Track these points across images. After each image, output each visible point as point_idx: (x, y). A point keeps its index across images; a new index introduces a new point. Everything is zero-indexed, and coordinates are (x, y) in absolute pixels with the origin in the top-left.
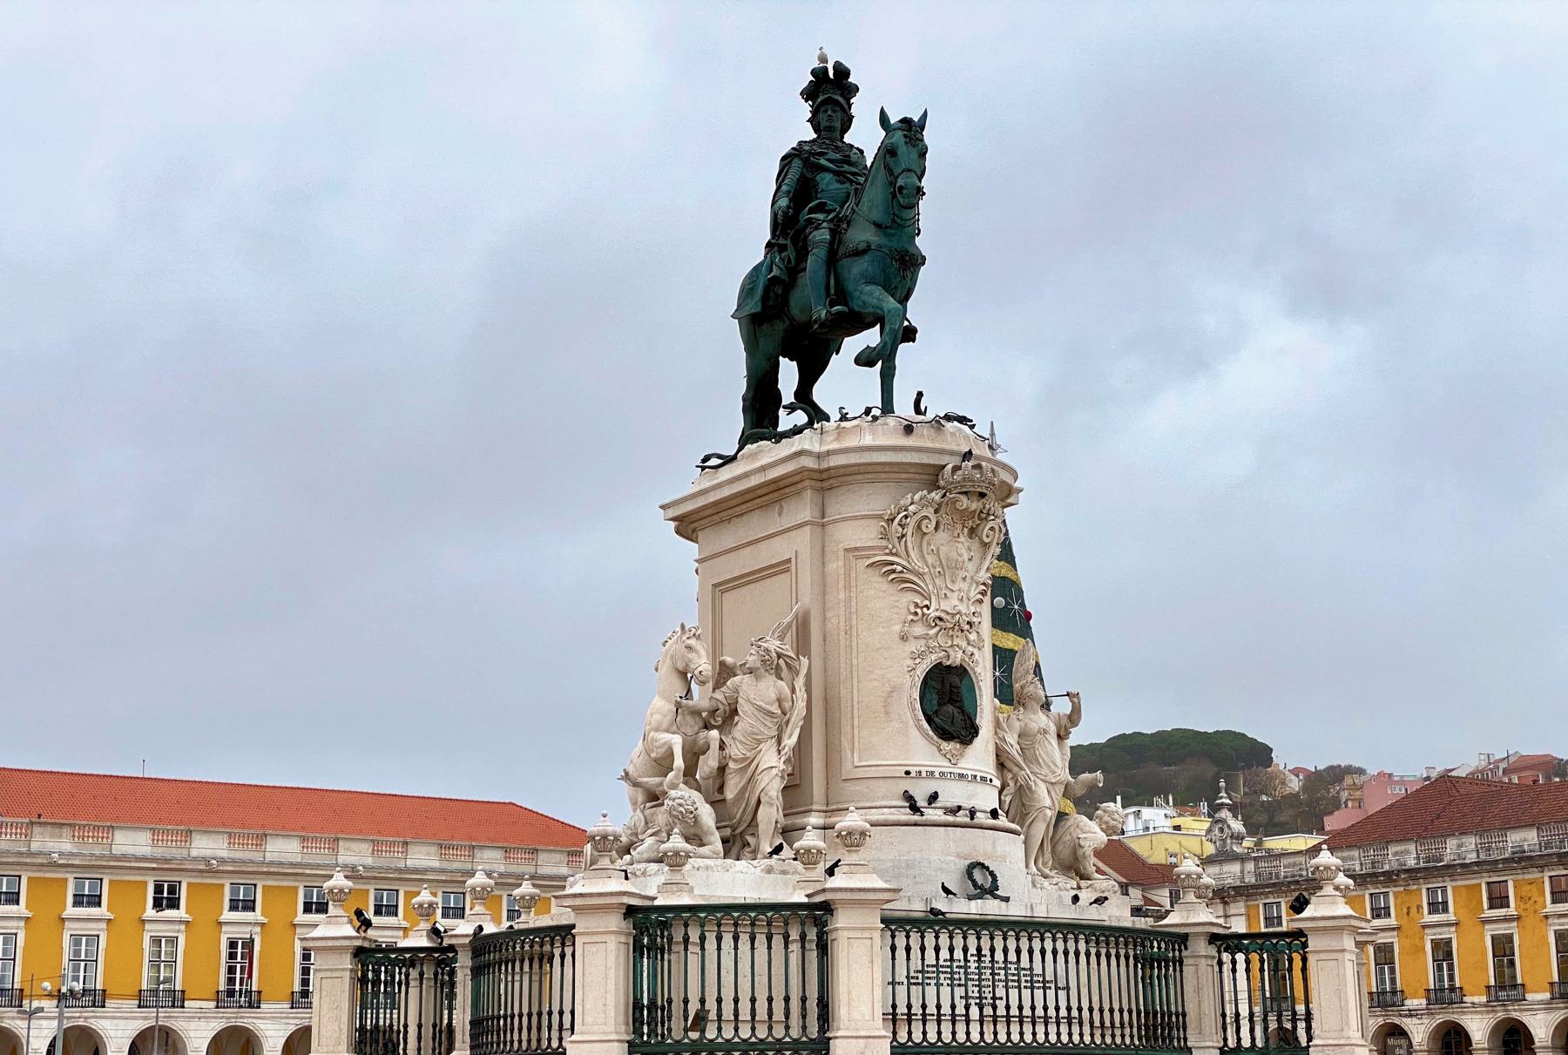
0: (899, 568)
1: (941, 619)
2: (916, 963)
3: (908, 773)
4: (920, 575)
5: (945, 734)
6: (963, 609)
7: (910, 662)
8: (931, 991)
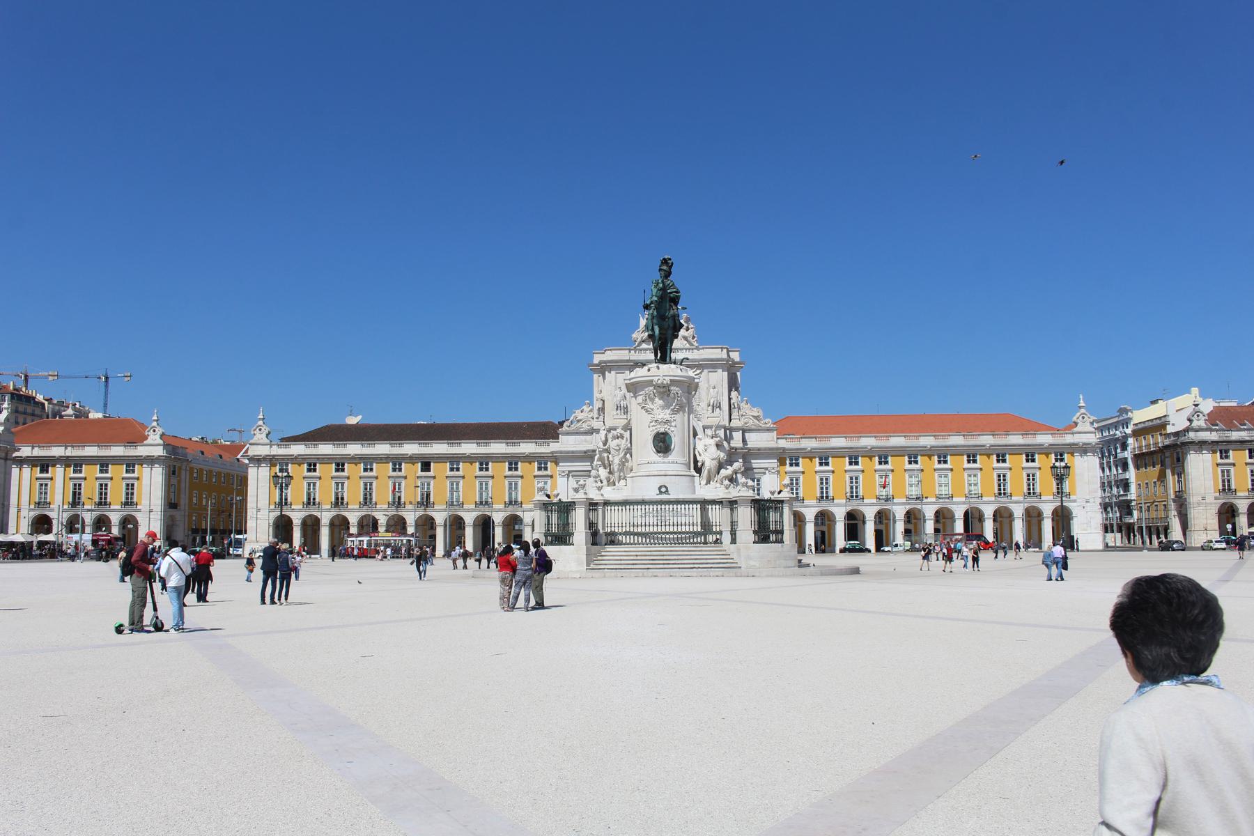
5: (658, 452)
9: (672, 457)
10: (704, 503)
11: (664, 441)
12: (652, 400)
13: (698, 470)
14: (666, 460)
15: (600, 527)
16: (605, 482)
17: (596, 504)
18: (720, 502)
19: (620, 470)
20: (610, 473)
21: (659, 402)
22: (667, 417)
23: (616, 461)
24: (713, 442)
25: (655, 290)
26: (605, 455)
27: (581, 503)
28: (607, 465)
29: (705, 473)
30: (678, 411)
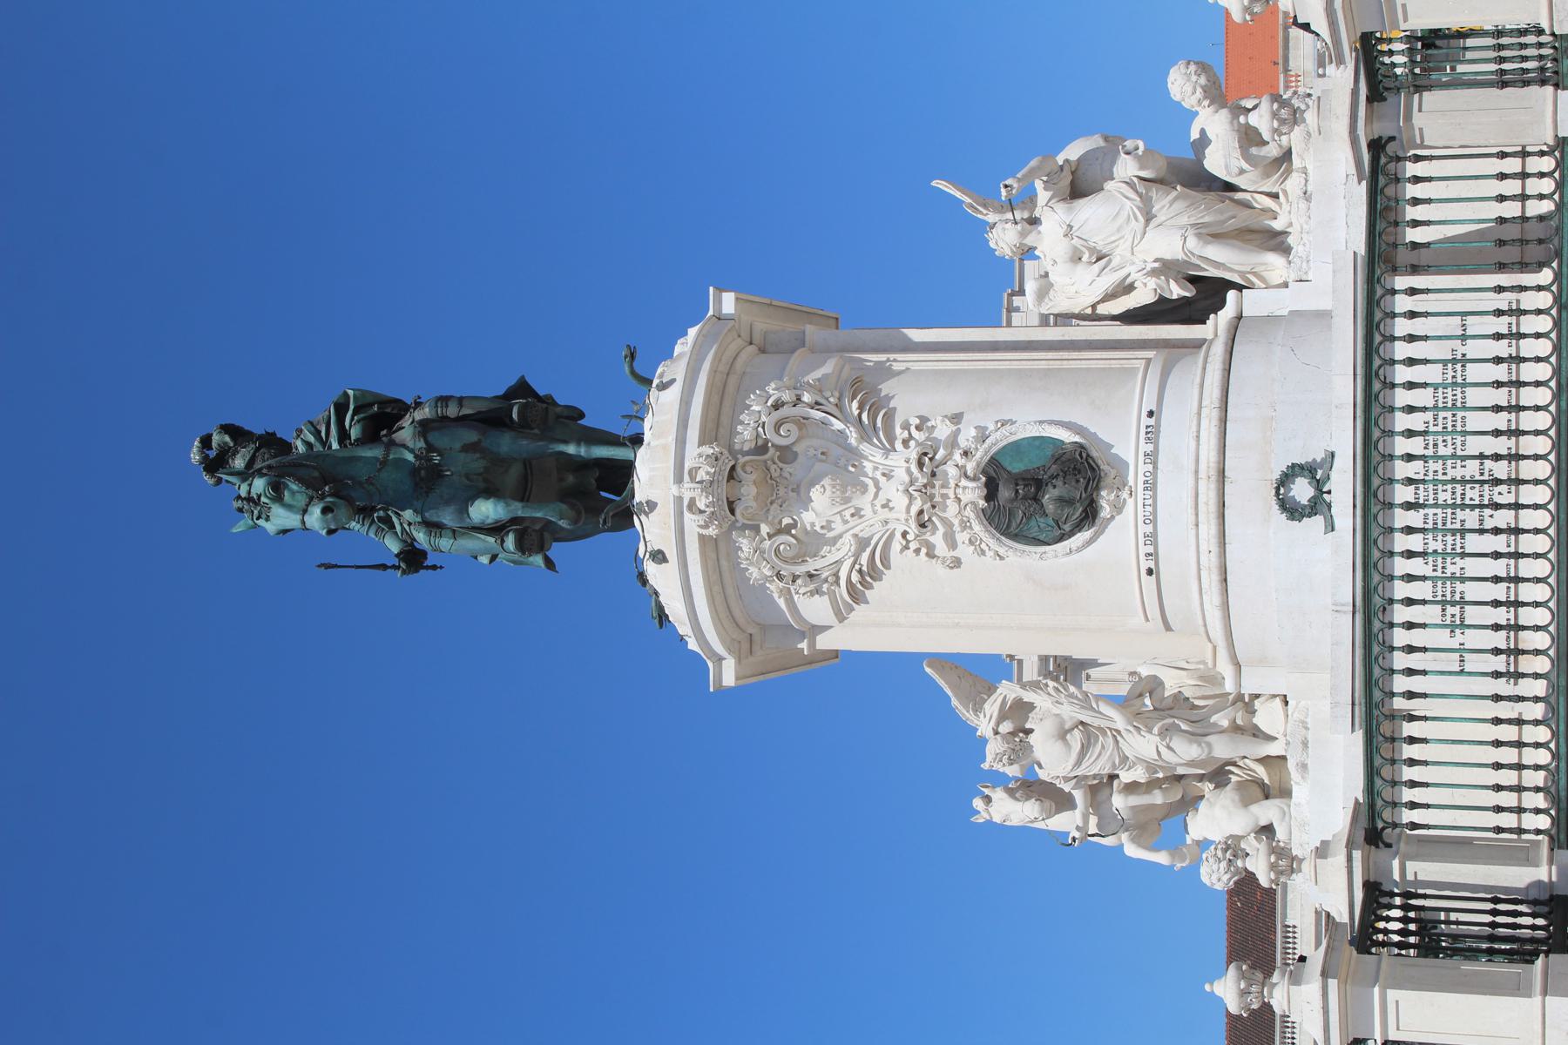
0: (855, 578)
1: (921, 512)
2: (1431, 614)
3: (1150, 572)
4: (862, 543)
5: (1090, 515)
6: (901, 475)
7: (990, 554)
8: (1473, 591)
9: (1120, 438)
10: (1386, 253)
11: (1033, 484)
12: (811, 543)
13: (1207, 295)
14: (1136, 474)
15: (1517, 877)
16: (1266, 812)
17: (1375, 894)
18: (1382, 164)
19: (1201, 729)
20: (1219, 775)
21: (818, 506)
22: (902, 462)
23: (1144, 745)
24: (1054, 218)
25: (281, 518)
26: (1119, 802)
27: (1354, 1009)
28: (1182, 791)
29: (1222, 260)
30: (875, 404)
